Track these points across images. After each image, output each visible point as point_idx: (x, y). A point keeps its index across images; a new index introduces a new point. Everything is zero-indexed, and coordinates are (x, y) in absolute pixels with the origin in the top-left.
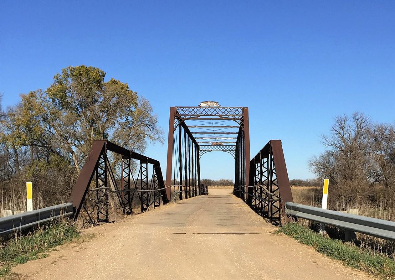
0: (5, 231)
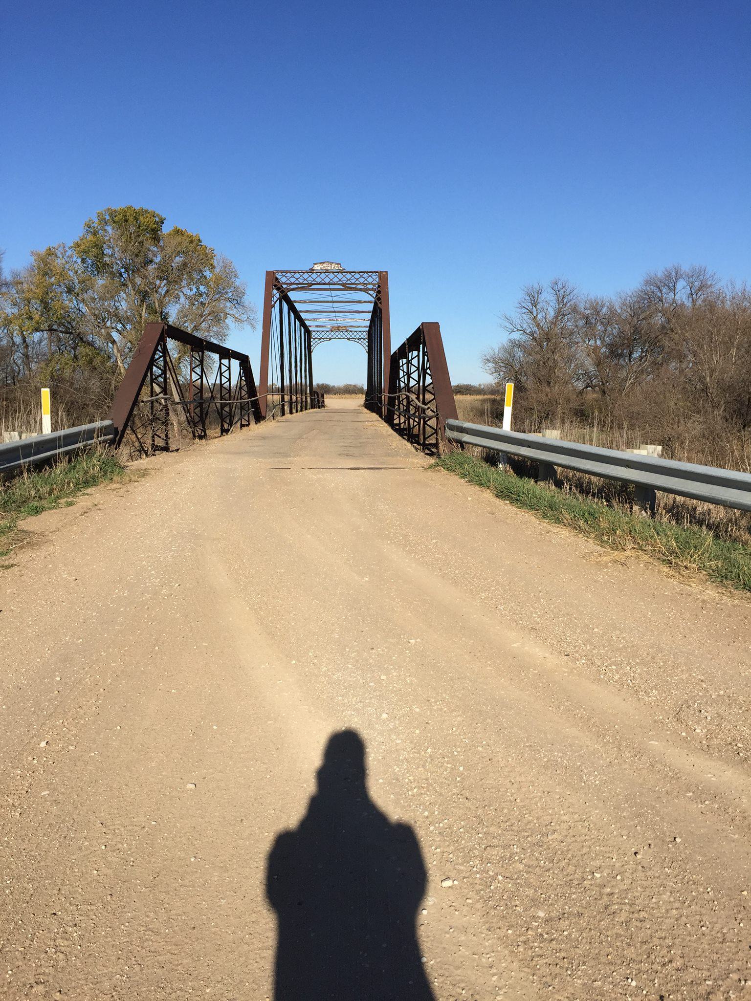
0: (9, 465)
